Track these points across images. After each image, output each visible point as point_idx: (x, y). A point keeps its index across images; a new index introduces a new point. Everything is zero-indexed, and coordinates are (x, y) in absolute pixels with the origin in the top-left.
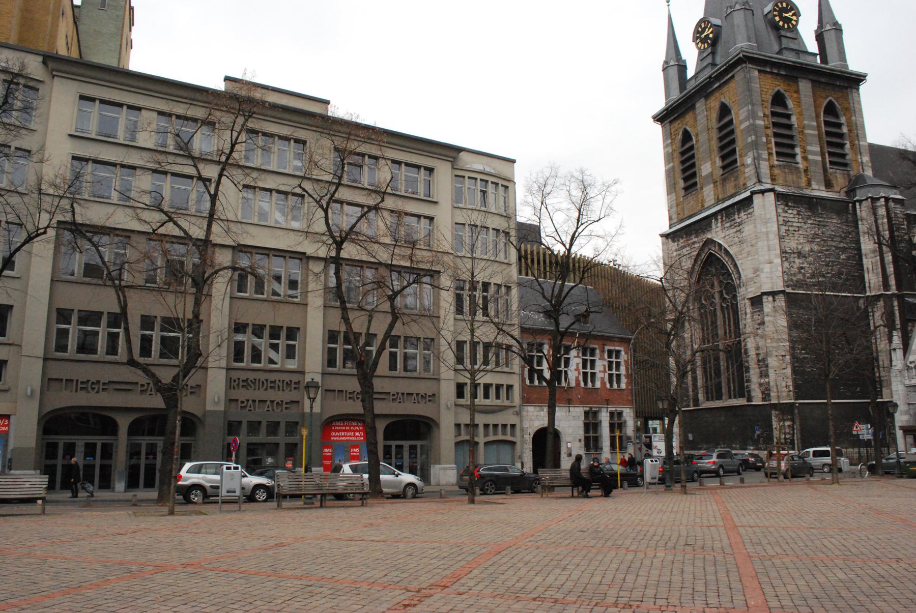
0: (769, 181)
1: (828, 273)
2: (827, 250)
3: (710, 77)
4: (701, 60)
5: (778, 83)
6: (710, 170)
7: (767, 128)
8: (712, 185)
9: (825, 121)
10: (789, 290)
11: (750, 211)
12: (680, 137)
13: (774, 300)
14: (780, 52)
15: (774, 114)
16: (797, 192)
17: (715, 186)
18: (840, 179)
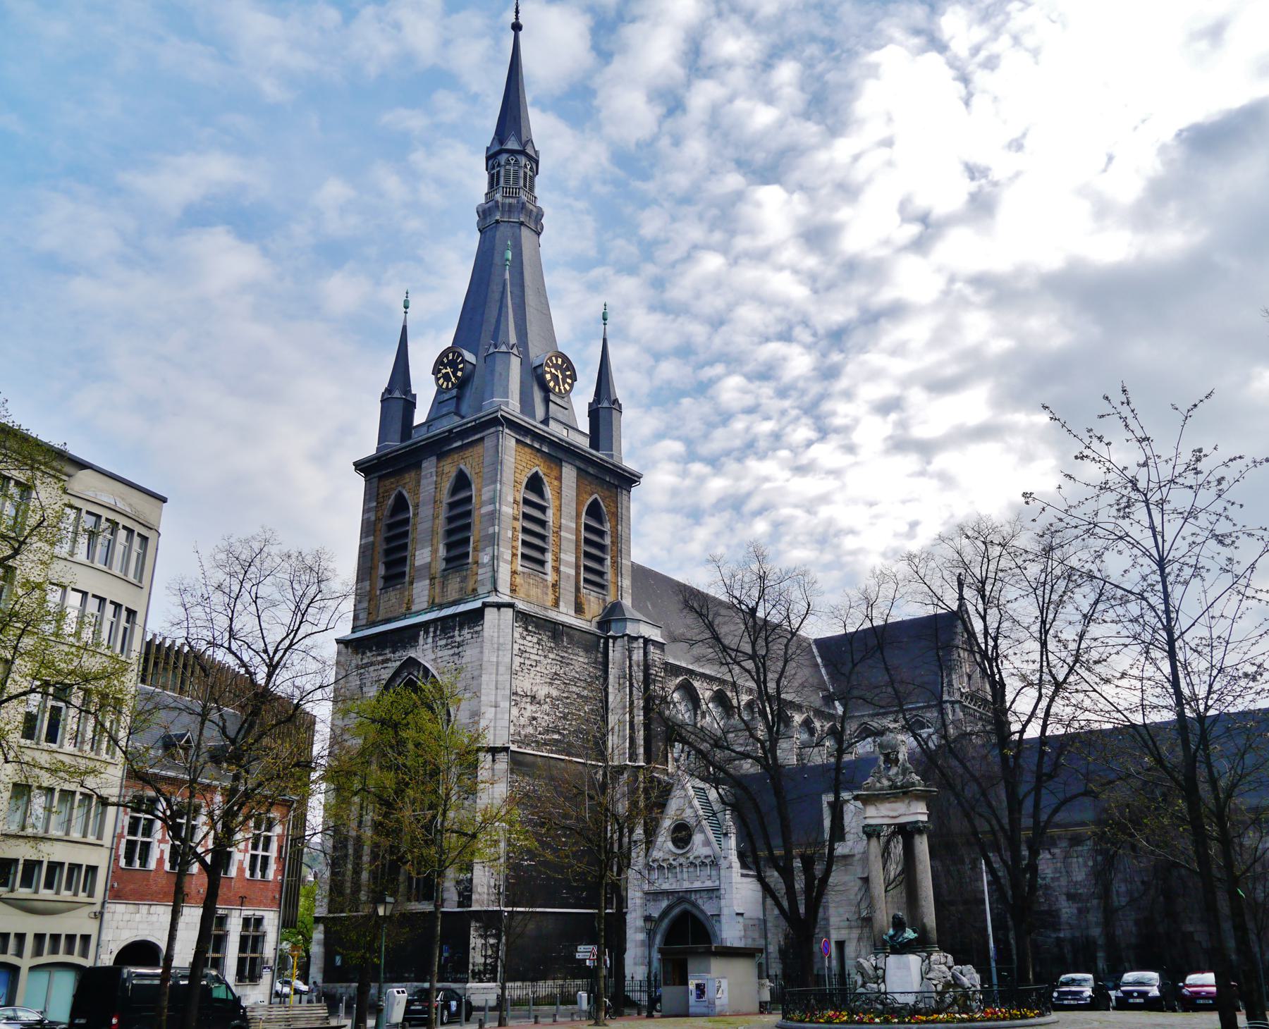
0: (508, 593)
1: (564, 729)
2: (567, 698)
3: (450, 431)
4: (438, 403)
5: (537, 462)
6: (428, 560)
7: (515, 519)
8: (427, 582)
9: (585, 524)
10: (514, 748)
11: (477, 629)
12: (391, 501)
13: (494, 760)
14: (545, 421)
15: (527, 502)
16: (540, 612)
17: (432, 585)
18: (594, 606)
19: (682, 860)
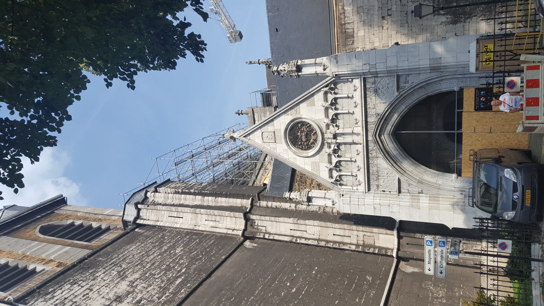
19: (329, 135)
